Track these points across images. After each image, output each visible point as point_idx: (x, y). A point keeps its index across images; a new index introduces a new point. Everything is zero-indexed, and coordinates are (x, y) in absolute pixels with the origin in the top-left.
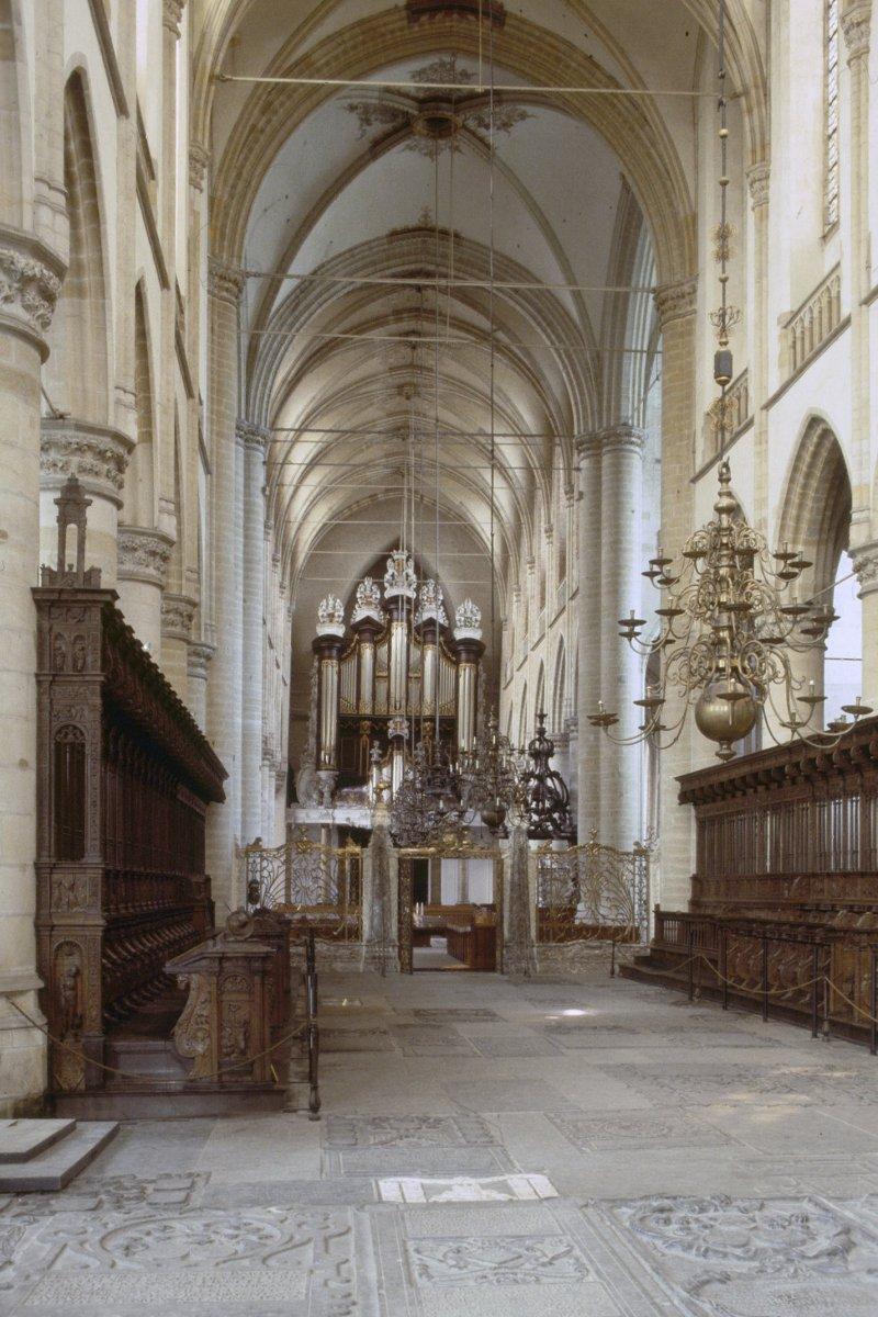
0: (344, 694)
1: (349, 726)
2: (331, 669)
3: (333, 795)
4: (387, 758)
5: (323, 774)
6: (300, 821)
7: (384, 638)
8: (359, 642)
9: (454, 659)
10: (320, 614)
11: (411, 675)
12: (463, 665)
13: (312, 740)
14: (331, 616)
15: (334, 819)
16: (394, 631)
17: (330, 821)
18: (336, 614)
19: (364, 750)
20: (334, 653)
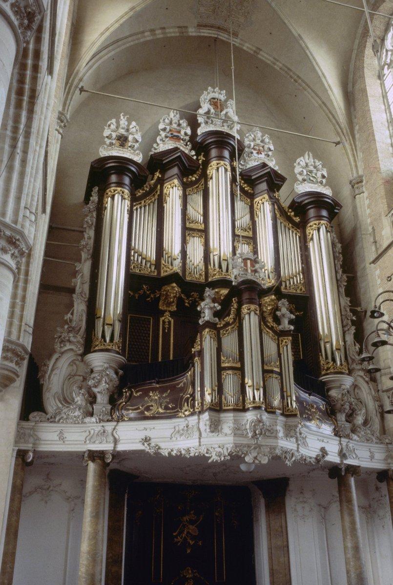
0: (137, 244)
1: (144, 287)
2: (118, 206)
3: (113, 401)
4: (230, 319)
5: (98, 360)
6: (44, 448)
7: (197, 181)
8: (161, 182)
9: (297, 219)
10: (106, 133)
11: (237, 232)
12: (313, 223)
13: (80, 307)
14: (123, 140)
15: (116, 442)
16: (211, 171)
17: (107, 447)
18: (130, 138)
19: (166, 336)
20: (127, 180)
